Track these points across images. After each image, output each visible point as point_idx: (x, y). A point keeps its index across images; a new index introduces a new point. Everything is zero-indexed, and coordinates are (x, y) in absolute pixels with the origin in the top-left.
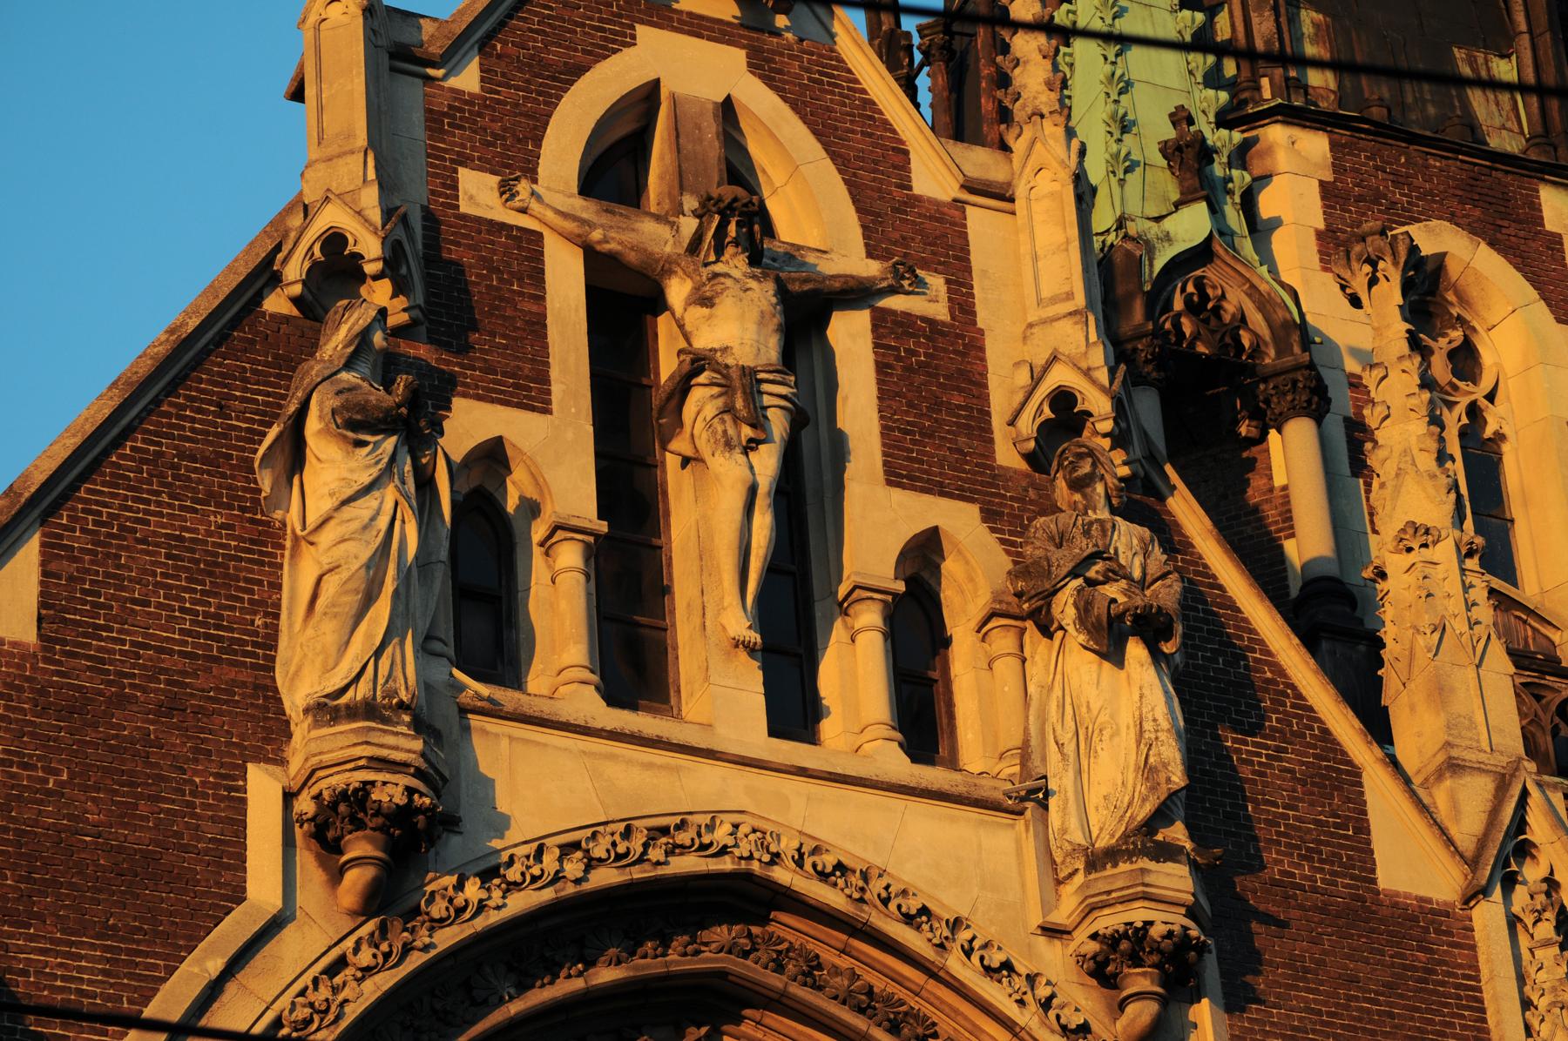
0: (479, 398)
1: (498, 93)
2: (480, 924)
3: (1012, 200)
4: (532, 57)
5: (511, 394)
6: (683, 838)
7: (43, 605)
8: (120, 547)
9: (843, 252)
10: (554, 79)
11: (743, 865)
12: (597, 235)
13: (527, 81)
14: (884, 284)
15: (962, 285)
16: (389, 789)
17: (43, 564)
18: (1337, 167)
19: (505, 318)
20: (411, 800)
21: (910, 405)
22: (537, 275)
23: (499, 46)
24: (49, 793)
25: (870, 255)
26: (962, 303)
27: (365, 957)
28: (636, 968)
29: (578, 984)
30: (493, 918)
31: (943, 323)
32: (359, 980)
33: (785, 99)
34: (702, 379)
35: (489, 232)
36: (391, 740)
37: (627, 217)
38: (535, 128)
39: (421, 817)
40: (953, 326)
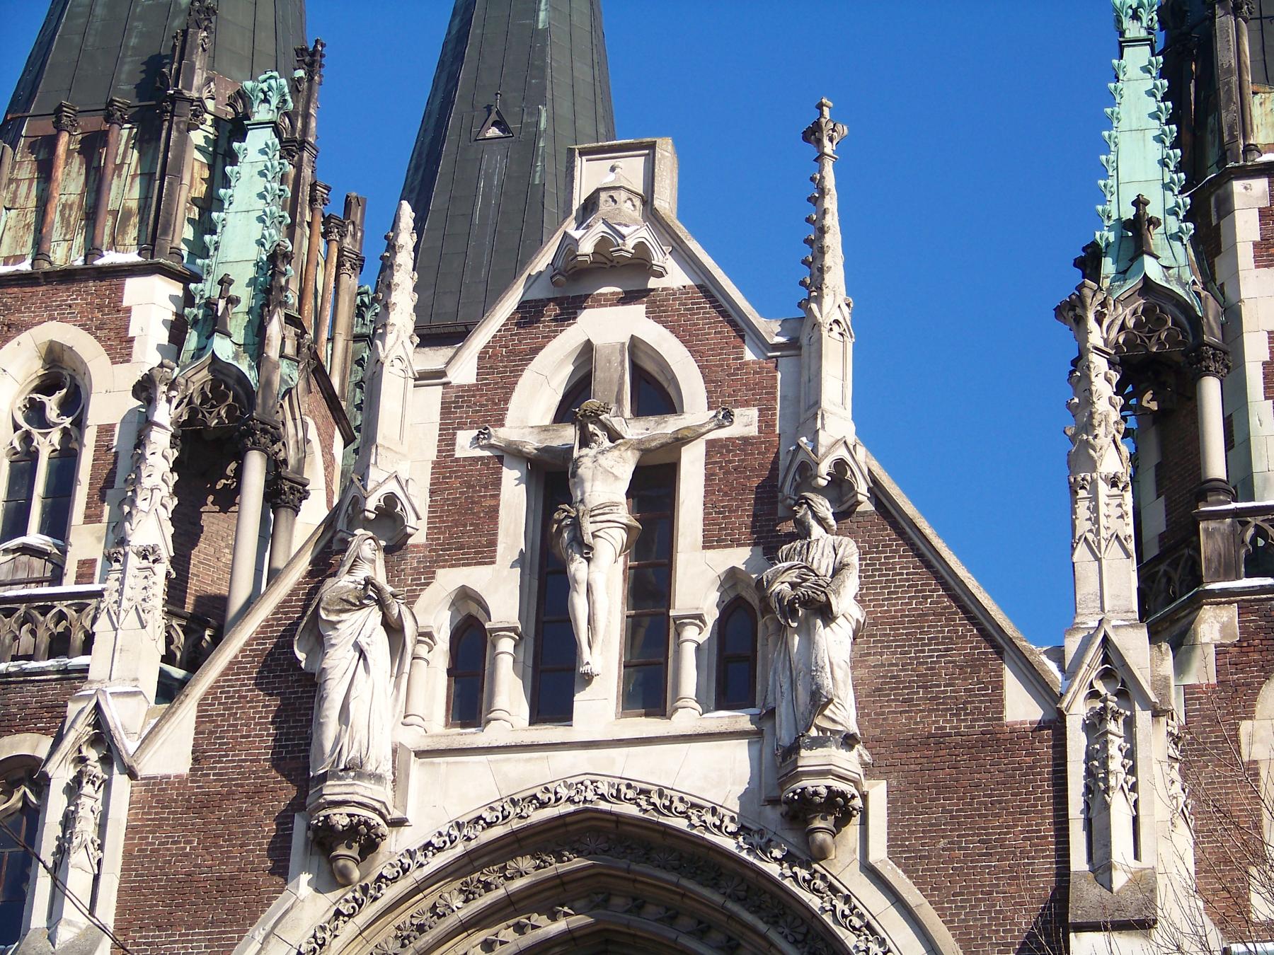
1: (487, 379)
4: (510, 351)
8: (238, 708)
9: (693, 412)
11: (581, 805)
13: (505, 367)
22: (497, 483)
24: (186, 855)
25: (710, 408)
30: (427, 870)
31: (754, 437)
35: (470, 465)
36: (337, 790)
37: (557, 430)
38: (507, 393)
40: (760, 437)
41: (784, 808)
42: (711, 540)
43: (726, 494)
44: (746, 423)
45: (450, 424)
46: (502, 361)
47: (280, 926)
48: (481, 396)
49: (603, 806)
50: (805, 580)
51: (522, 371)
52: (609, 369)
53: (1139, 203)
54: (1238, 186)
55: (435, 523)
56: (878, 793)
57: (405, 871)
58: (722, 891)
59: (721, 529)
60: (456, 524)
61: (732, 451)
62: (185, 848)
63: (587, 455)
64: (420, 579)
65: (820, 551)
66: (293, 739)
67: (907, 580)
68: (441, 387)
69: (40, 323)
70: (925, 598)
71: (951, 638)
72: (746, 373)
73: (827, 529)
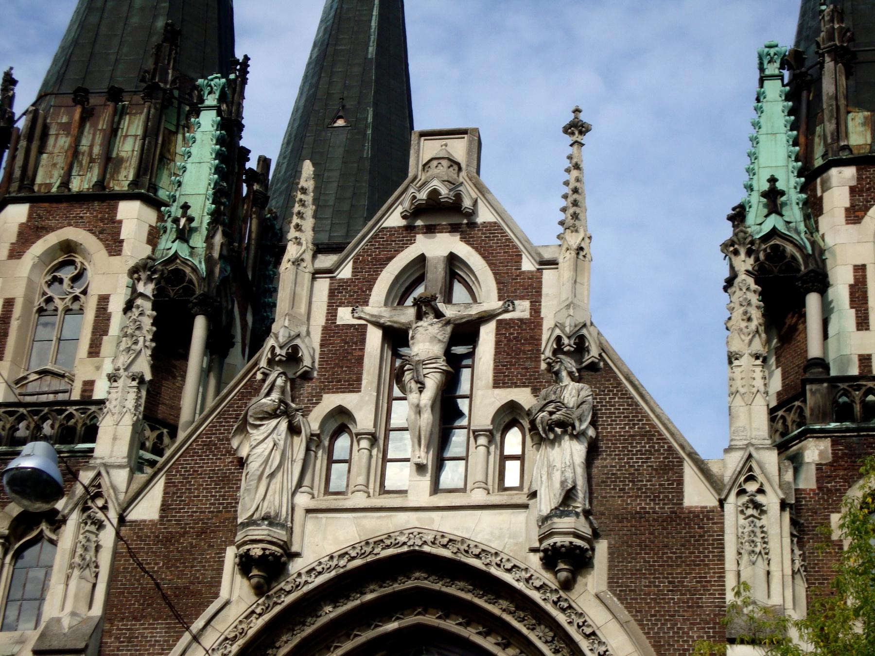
0: (333, 393)
2: (306, 589)
3: (557, 264)
4: (373, 258)
5: (346, 388)
6: (388, 542)
7: (162, 505)
8: (192, 478)
10: (380, 265)
11: (412, 548)
12: (382, 321)
13: (370, 268)
14: (501, 310)
15: (537, 302)
16: (256, 550)
17: (164, 490)
18: (859, 179)
19: (348, 360)
20: (264, 553)
21: (508, 354)
22: (363, 341)
23: (361, 258)
25: (499, 300)
26: (536, 309)
27: (258, 611)
28: (381, 592)
29: (358, 602)
30: (311, 586)
31: (526, 319)
32: (257, 619)
33: (473, 248)
34: (405, 368)
35: (346, 329)
38: (371, 285)
39: (270, 557)
40: (530, 319)
41: (542, 554)
42: (499, 382)
43: (508, 354)
44: (522, 309)
45: (334, 303)
46: (368, 265)
47: (214, 620)
48: (355, 286)
49: (426, 549)
50: (559, 410)
51: (381, 271)
52: (436, 272)
53: (773, 180)
54: (834, 171)
55: (323, 365)
56: (602, 548)
57: (297, 586)
58: (500, 607)
59: (505, 376)
60: (337, 365)
61: (513, 327)
62: (154, 568)
63: (421, 326)
64: (312, 400)
65: (569, 392)
66: (228, 499)
67: (623, 413)
68: (328, 279)
69: (61, 228)
70: (634, 425)
71: (650, 451)
72: (524, 279)
73: (573, 379)
